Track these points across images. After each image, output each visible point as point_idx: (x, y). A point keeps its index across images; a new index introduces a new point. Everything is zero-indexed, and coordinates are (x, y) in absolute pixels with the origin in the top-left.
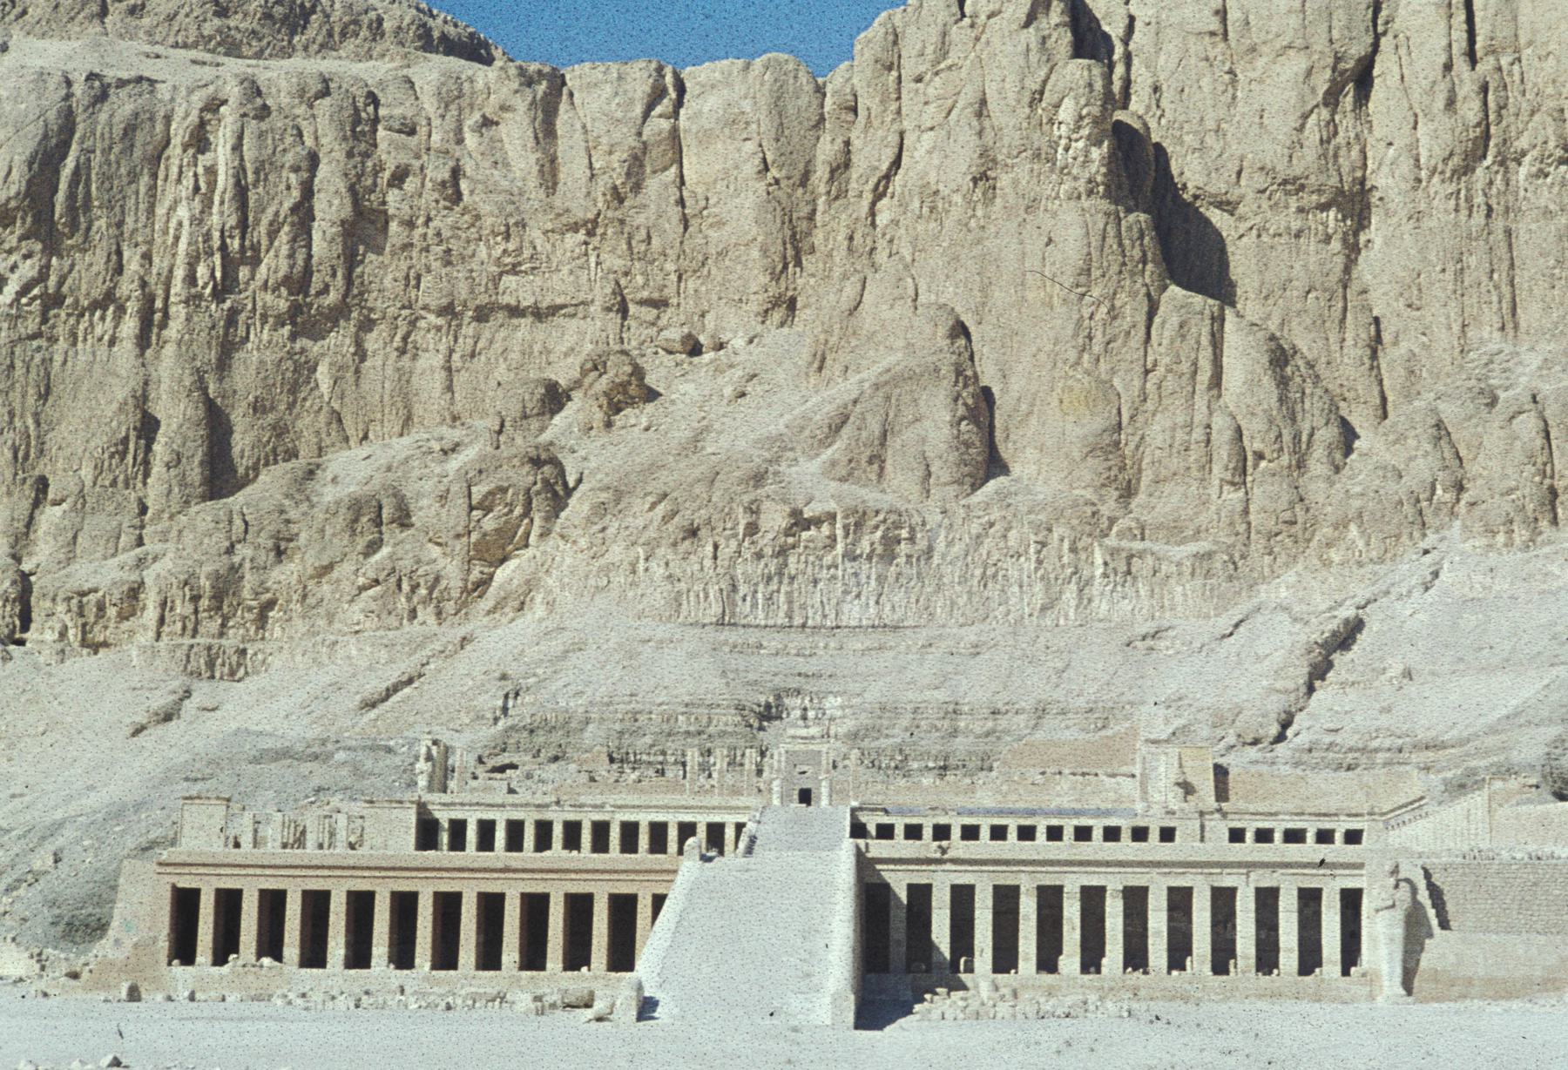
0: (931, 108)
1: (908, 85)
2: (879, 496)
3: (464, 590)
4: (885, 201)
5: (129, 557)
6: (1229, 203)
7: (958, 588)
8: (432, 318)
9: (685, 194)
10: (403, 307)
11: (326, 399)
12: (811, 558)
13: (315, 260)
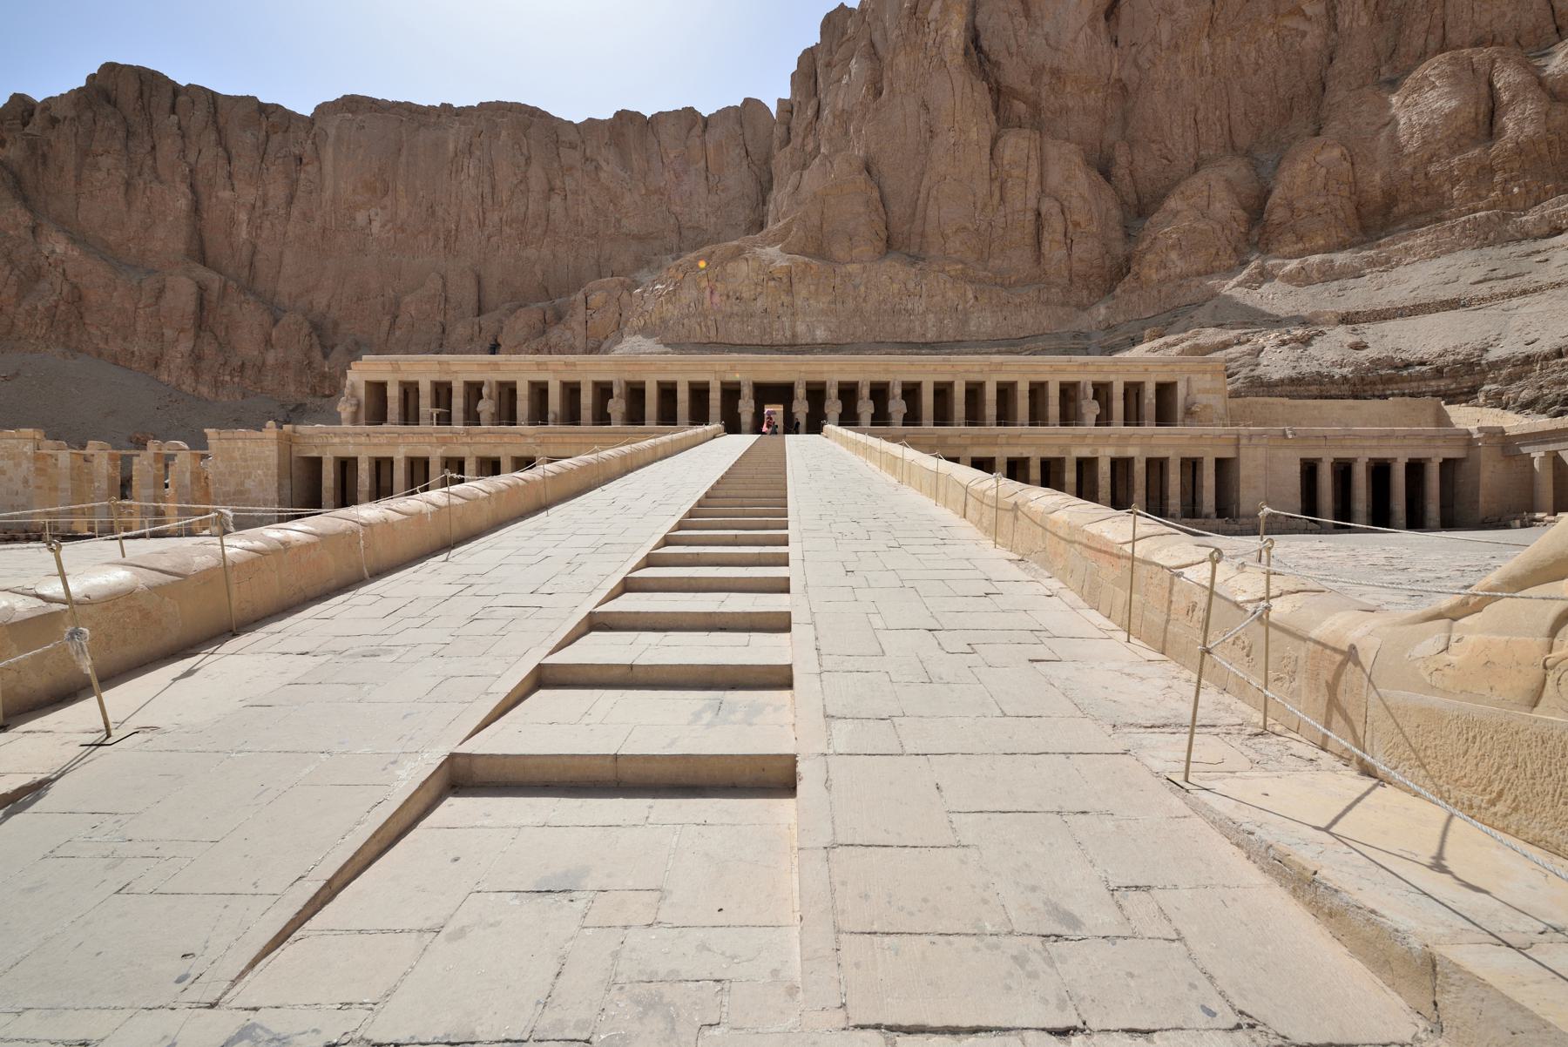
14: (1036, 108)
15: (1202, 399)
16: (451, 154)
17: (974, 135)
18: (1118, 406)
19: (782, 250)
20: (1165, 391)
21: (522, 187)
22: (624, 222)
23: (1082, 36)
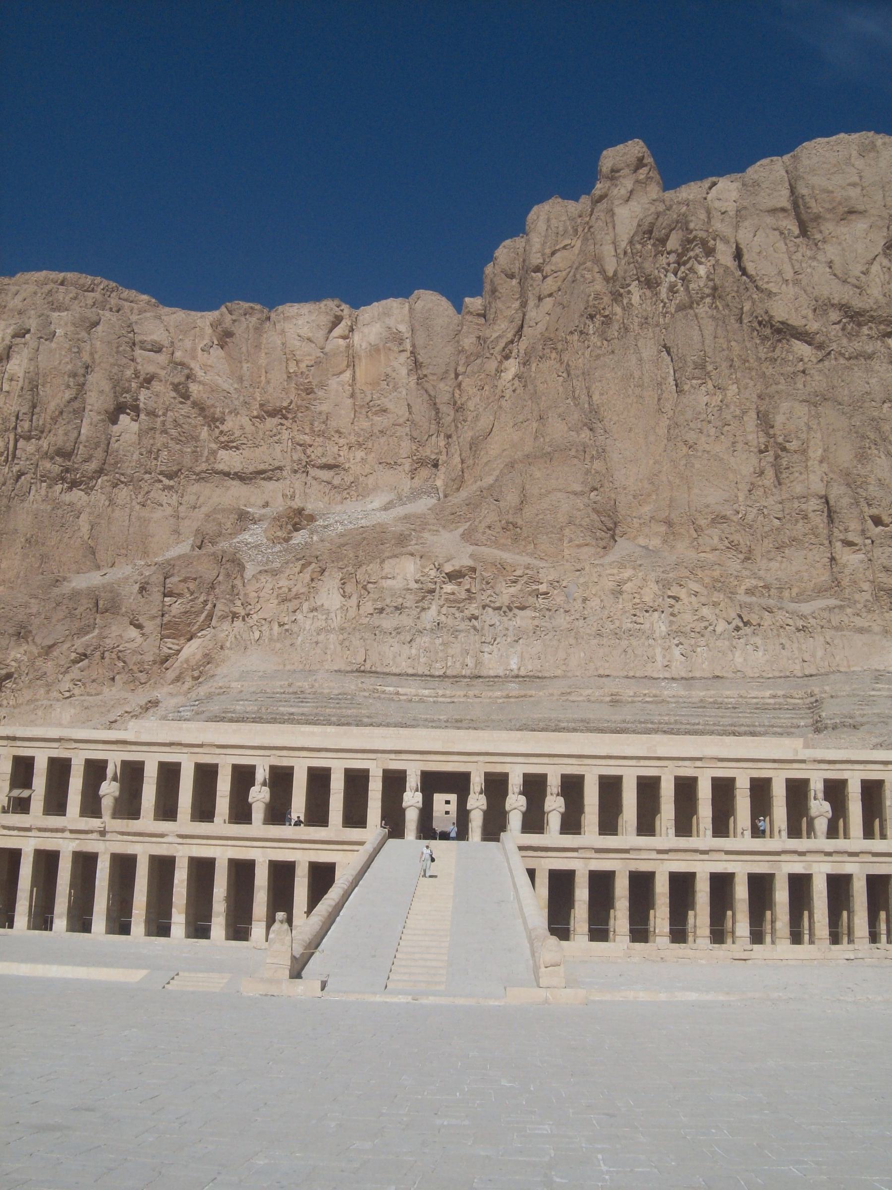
0: (549, 280)
2: (517, 557)
3: (155, 662)
4: (511, 360)
6: (807, 333)
7: (594, 642)
8: (166, 481)
9: (357, 391)
10: (146, 473)
11: (86, 537)
12: (453, 610)
13: (83, 438)
19: (463, 535)
21: (76, 405)
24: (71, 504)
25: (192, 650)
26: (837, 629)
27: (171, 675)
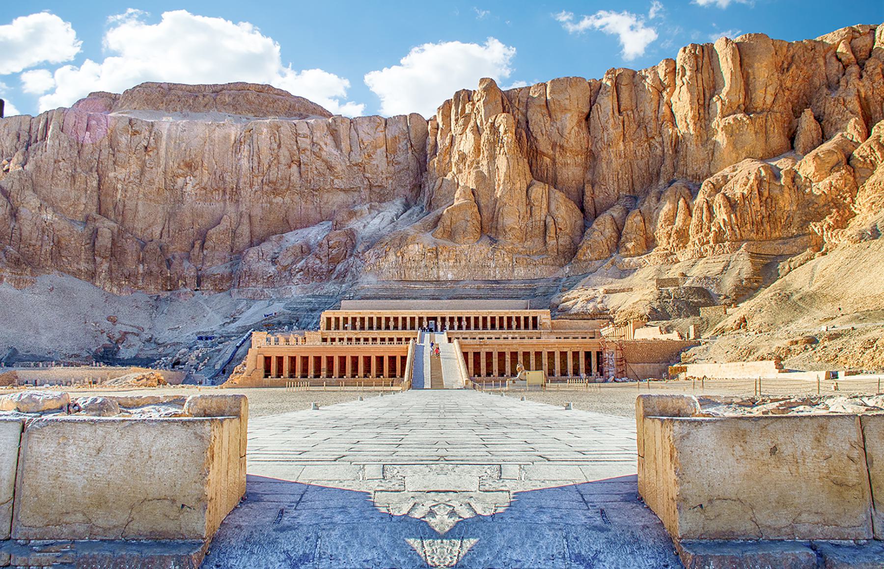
1: (453, 122)
5: (228, 265)
14: (554, 161)
15: (544, 321)
16: (232, 142)
17: (518, 185)
18: (522, 323)
20: (535, 319)
21: (275, 162)
22: (336, 181)
23: (573, 131)
24: (277, 203)
25: (340, 267)
26: (546, 264)
27: (333, 277)
